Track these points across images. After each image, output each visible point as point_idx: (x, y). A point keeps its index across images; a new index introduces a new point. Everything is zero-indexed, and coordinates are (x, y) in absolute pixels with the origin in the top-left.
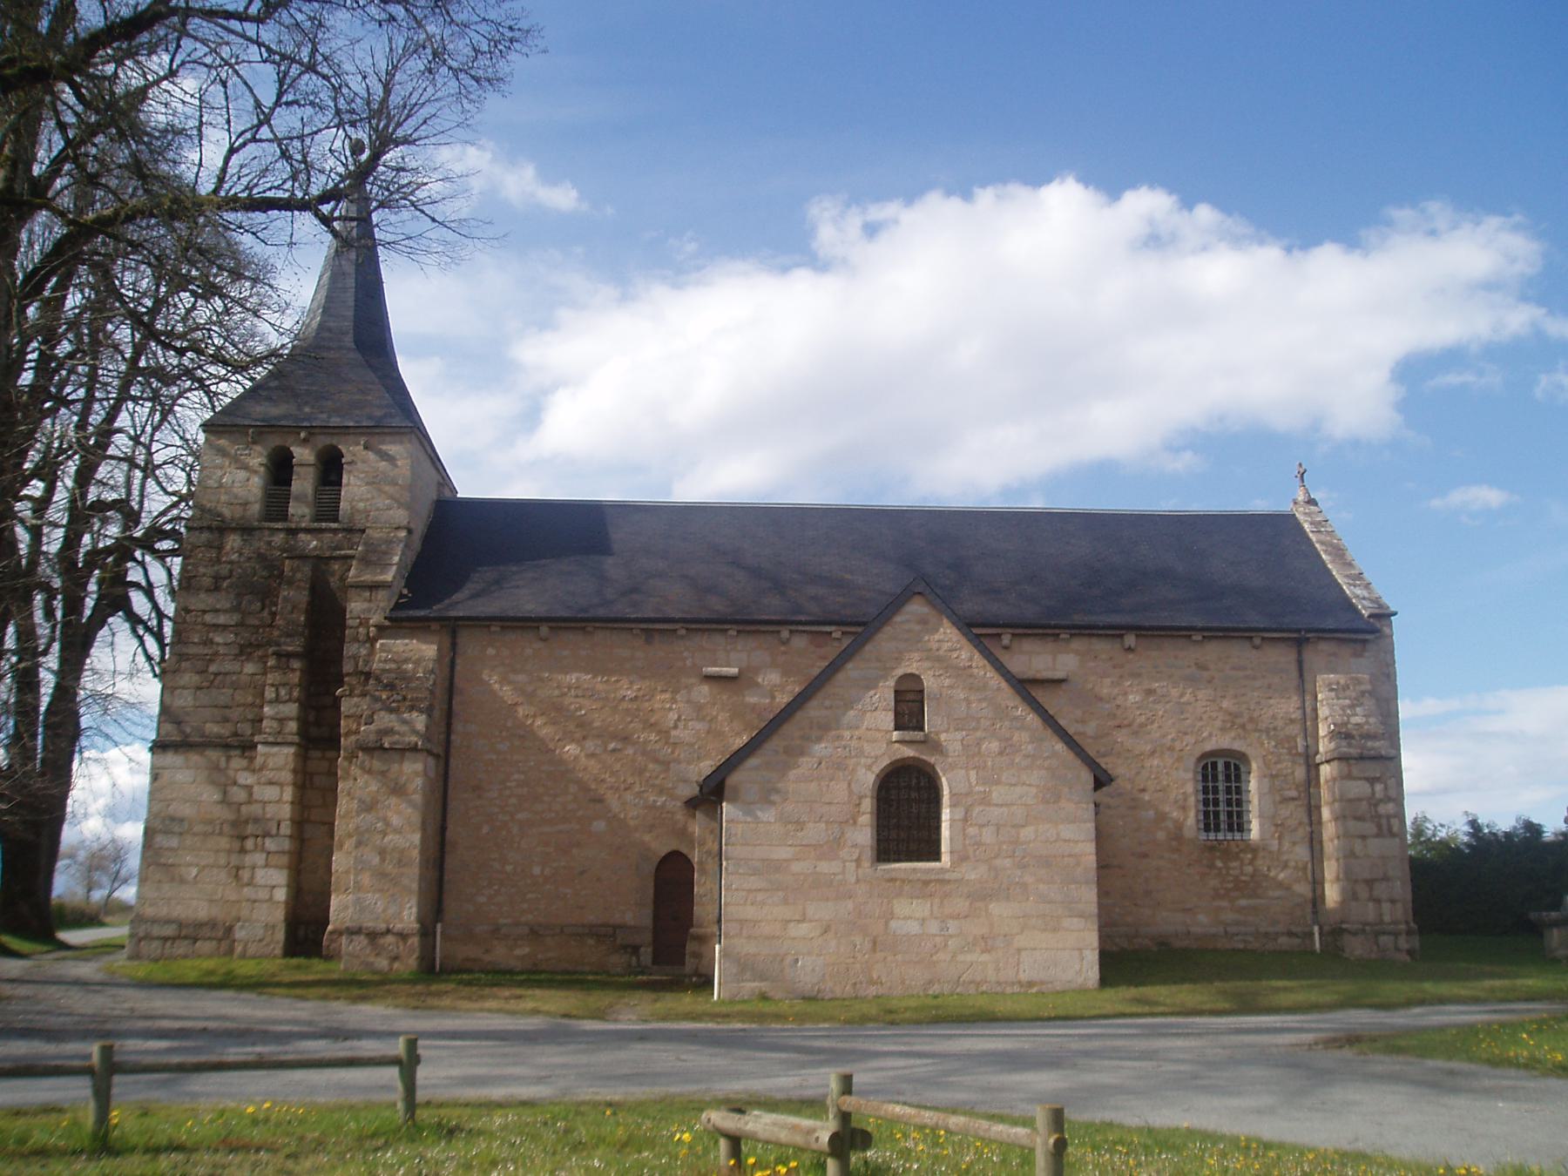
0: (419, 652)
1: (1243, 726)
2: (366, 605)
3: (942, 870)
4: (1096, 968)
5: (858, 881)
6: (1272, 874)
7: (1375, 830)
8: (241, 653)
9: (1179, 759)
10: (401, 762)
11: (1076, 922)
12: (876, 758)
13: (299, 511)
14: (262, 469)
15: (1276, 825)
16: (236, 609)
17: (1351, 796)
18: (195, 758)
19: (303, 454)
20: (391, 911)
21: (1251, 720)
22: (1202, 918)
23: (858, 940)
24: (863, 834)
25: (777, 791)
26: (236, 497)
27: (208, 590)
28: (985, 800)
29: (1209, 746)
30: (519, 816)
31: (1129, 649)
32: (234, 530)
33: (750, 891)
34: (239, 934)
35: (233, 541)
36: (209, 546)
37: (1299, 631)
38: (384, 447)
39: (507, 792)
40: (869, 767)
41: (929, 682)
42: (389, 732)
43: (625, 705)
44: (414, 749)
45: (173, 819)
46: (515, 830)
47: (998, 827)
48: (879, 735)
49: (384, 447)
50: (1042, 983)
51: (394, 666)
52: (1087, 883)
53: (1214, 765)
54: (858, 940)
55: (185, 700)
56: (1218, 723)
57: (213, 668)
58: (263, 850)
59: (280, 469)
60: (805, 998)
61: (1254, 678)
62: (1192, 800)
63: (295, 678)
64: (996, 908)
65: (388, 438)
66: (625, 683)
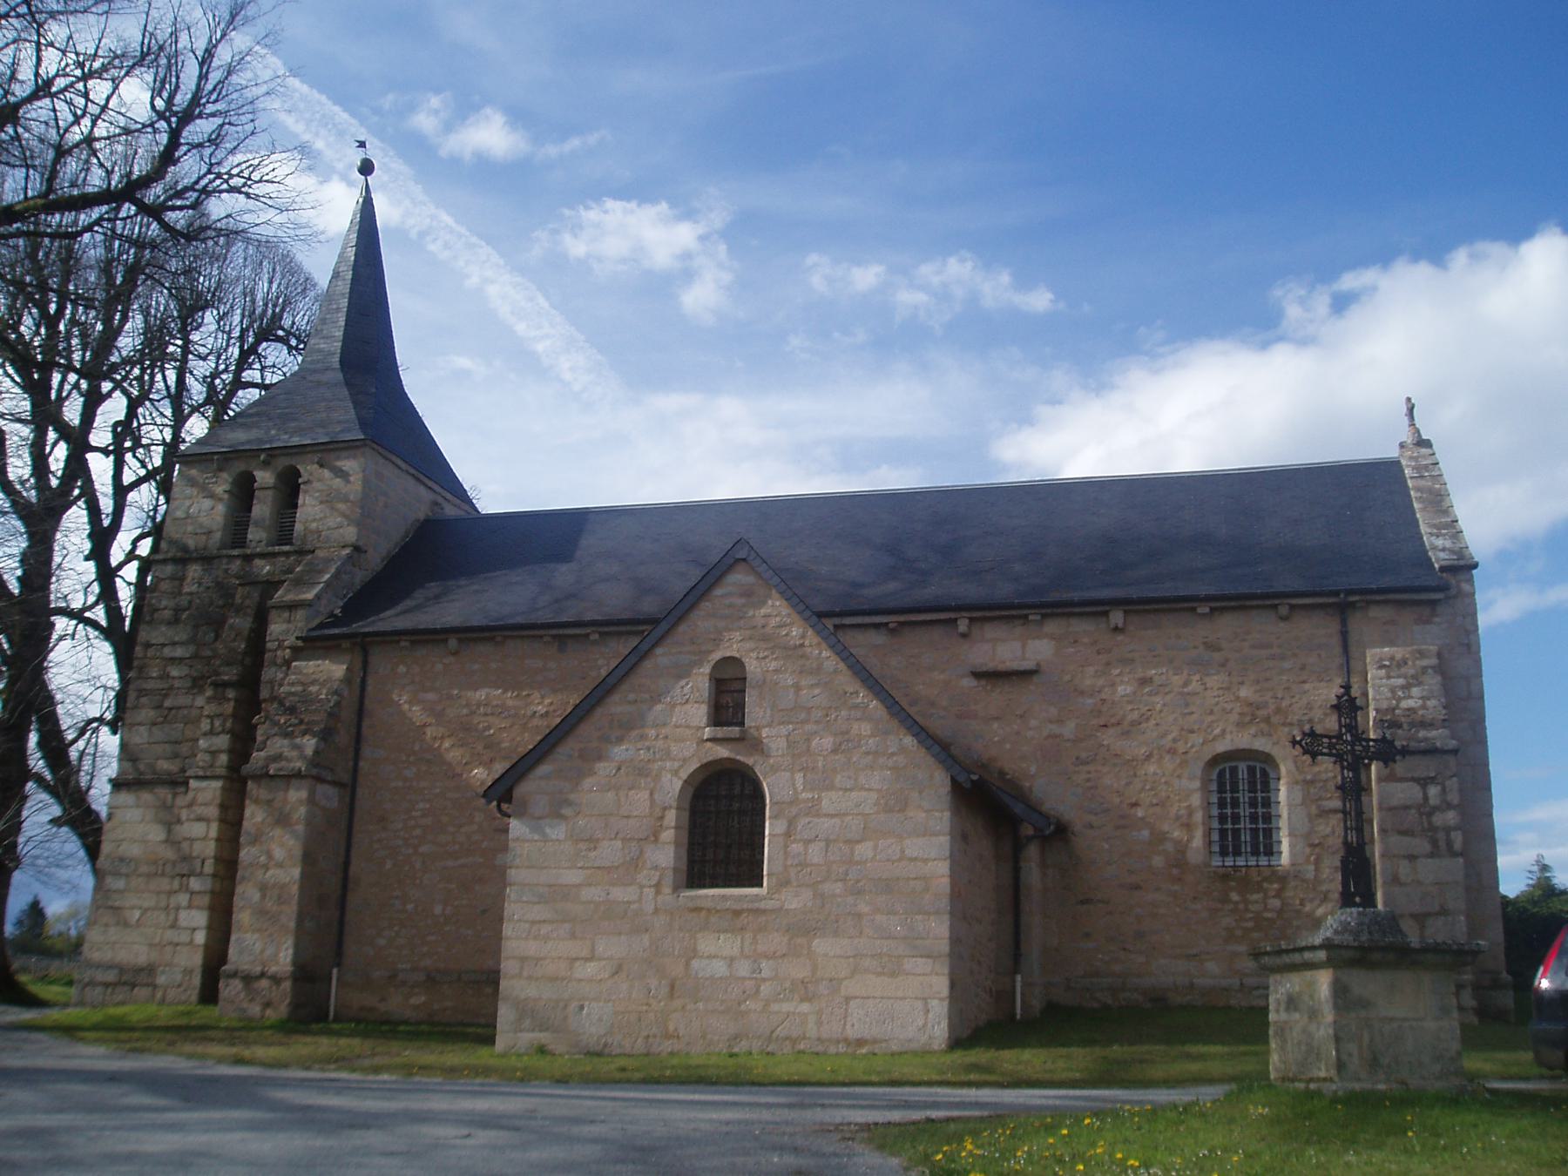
0: (330, 670)
1: (1267, 720)
2: (285, 626)
3: (757, 898)
4: (944, 1024)
5: (656, 911)
6: (1308, 908)
7: (1427, 847)
8: (193, 687)
9: (1183, 764)
10: (287, 790)
11: (922, 965)
12: (684, 760)
13: (255, 535)
14: (226, 496)
15: (1313, 846)
16: (192, 640)
17: (1394, 802)
18: (146, 796)
19: (264, 477)
20: (268, 953)
21: (1278, 710)
22: (1212, 966)
23: (653, 983)
24: (665, 855)
25: (569, 803)
26: (201, 526)
27: (169, 623)
28: (813, 810)
29: (1222, 747)
30: (423, 849)
31: (1116, 629)
32: (196, 560)
33: (533, 923)
34: (161, 980)
35: (194, 571)
36: (172, 578)
37: (1336, 594)
38: (339, 464)
39: (413, 822)
40: (676, 773)
41: (752, 666)
42: (278, 757)
43: (536, 722)
44: (298, 775)
45: (122, 859)
46: (418, 865)
47: (828, 842)
48: (688, 732)
49: (339, 464)
50: (875, 1041)
51: (300, 688)
52: (937, 913)
53: (1234, 770)
54: (653, 983)
55: (140, 737)
56: (1234, 717)
57: (167, 703)
58: (187, 890)
59: (244, 492)
60: (589, 1054)
61: (1283, 658)
62: (1199, 816)
63: (229, 708)
64: (821, 945)
65: (344, 454)
66: (536, 695)
